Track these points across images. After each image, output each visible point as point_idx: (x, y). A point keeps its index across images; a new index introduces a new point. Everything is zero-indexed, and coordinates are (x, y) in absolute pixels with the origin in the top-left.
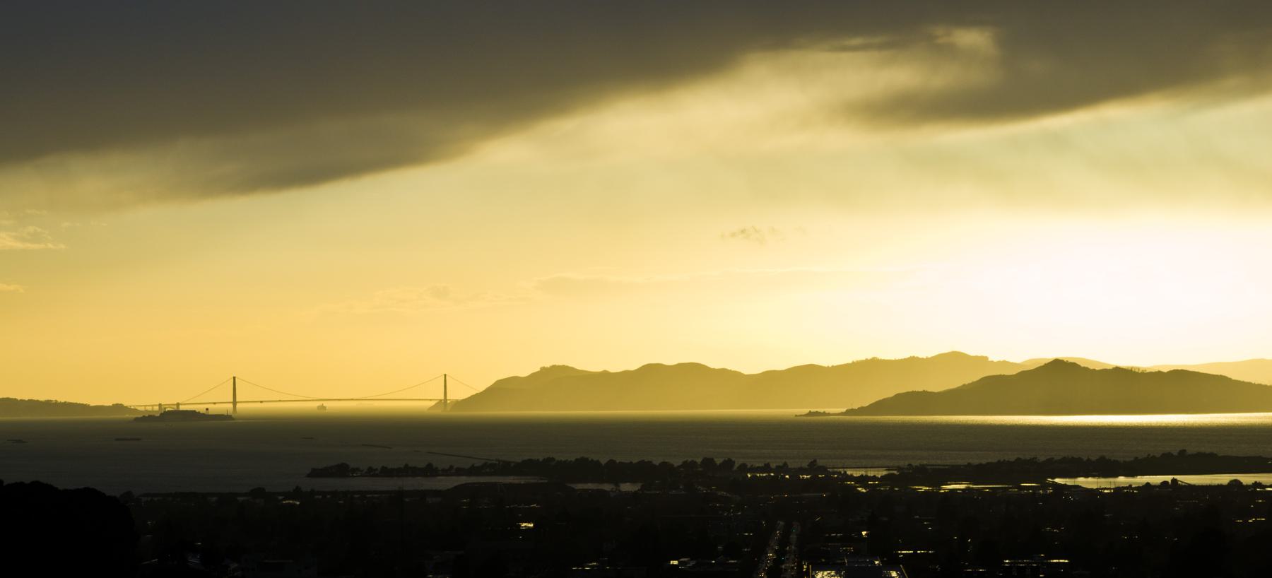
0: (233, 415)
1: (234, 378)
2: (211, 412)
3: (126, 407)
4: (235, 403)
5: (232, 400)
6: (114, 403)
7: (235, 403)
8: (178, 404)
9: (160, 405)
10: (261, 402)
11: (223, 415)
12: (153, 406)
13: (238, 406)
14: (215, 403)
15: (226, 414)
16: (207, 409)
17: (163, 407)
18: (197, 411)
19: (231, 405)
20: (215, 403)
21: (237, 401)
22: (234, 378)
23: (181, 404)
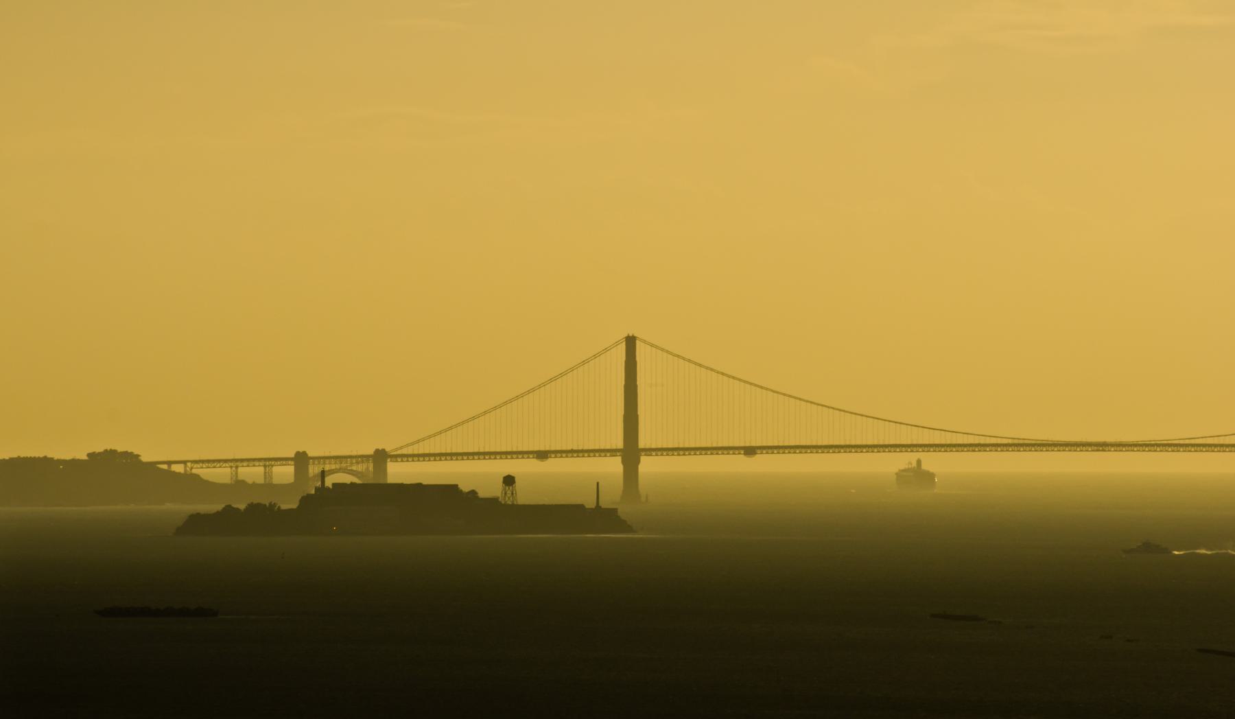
0: (624, 511)
2: (524, 495)
3: (153, 464)
4: (631, 453)
5: (619, 443)
6: (99, 449)
7: (631, 453)
8: (381, 457)
9: (301, 460)
10: (750, 451)
11: (580, 507)
12: (268, 462)
13: (648, 466)
14: (542, 455)
15: (590, 503)
16: (509, 480)
17: (314, 470)
18: (465, 487)
19: (614, 466)
20: (542, 455)
21: (643, 442)
22: (631, 342)
23: (395, 458)
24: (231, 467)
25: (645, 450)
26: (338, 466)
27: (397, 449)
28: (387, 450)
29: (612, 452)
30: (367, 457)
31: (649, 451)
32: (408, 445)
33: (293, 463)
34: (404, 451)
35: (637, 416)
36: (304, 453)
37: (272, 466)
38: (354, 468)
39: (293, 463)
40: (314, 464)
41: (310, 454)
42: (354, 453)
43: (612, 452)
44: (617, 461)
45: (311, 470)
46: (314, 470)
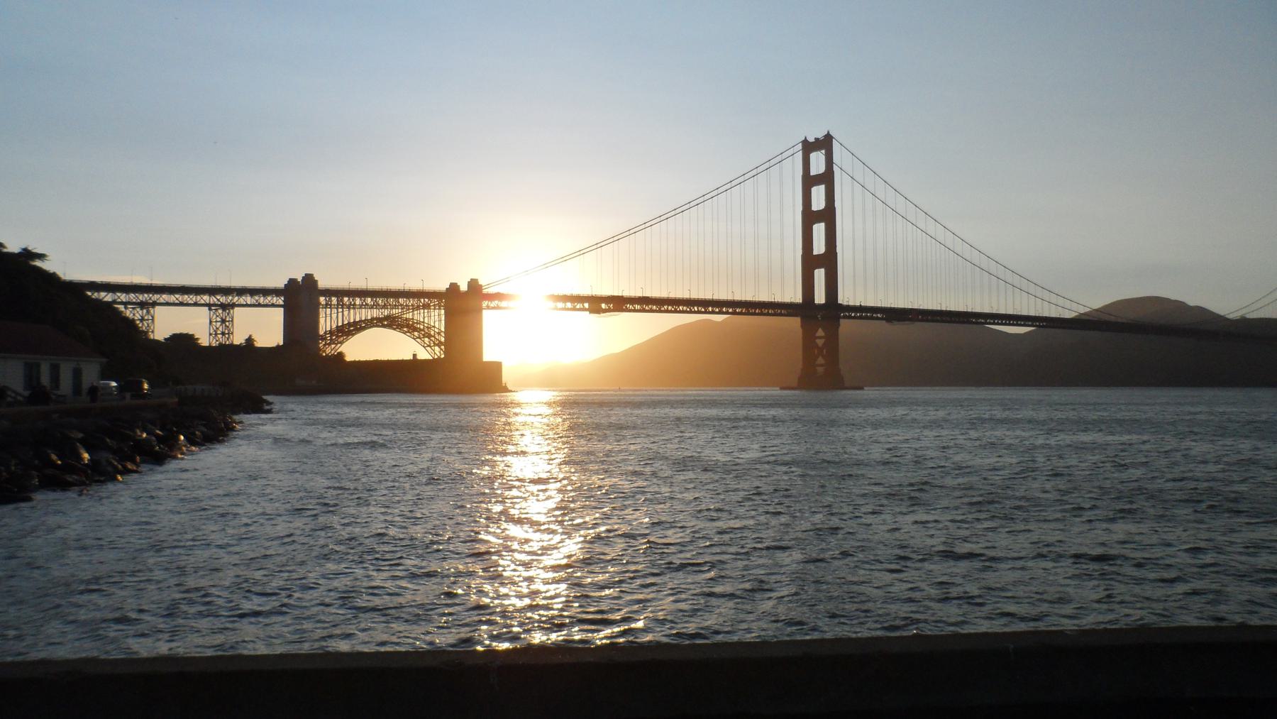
17: (327, 321)
33: (280, 301)
39: (282, 303)
40: (328, 305)
41: (323, 283)
45: (322, 321)
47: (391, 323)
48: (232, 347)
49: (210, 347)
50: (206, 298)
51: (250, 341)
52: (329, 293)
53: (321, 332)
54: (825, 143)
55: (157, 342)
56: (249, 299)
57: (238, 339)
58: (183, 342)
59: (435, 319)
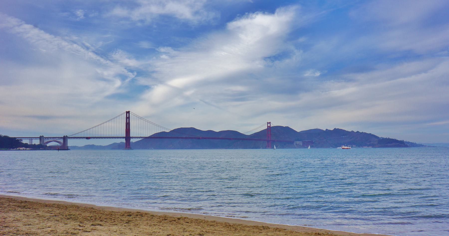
1: (128, 112)
4: (128, 137)
5: (125, 136)
7: (128, 137)
8: (65, 138)
9: (41, 138)
12: (31, 138)
19: (124, 141)
21: (131, 136)
24: (29, 139)
25: (131, 137)
26: (52, 140)
27: (70, 136)
28: (68, 136)
29: (123, 138)
30: (62, 137)
31: (133, 137)
32: (73, 135)
33: (39, 139)
34: (72, 137)
35: (130, 129)
36: (43, 136)
37: (32, 139)
38: (58, 140)
39: (39, 139)
40: (46, 139)
42: (58, 136)
43: (123, 138)
44: (125, 139)
46: (46, 141)
47: (55, 141)
48: (32, 145)
49: (29, 145)
50: (29, 139)
51: (35, 144)
52: (46, 138)
53: (45, 142)
54: (128, 112)
55: (23, 143)
56: (35, 139)
57: (33, 144)
58: (26, 144)
59: (62, 141)
